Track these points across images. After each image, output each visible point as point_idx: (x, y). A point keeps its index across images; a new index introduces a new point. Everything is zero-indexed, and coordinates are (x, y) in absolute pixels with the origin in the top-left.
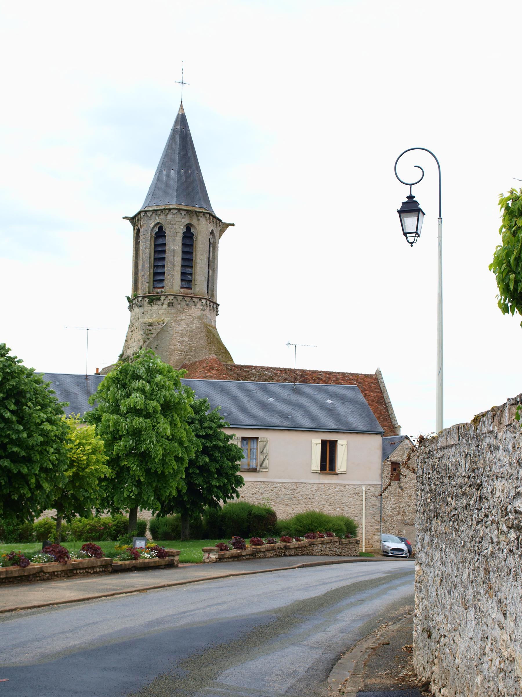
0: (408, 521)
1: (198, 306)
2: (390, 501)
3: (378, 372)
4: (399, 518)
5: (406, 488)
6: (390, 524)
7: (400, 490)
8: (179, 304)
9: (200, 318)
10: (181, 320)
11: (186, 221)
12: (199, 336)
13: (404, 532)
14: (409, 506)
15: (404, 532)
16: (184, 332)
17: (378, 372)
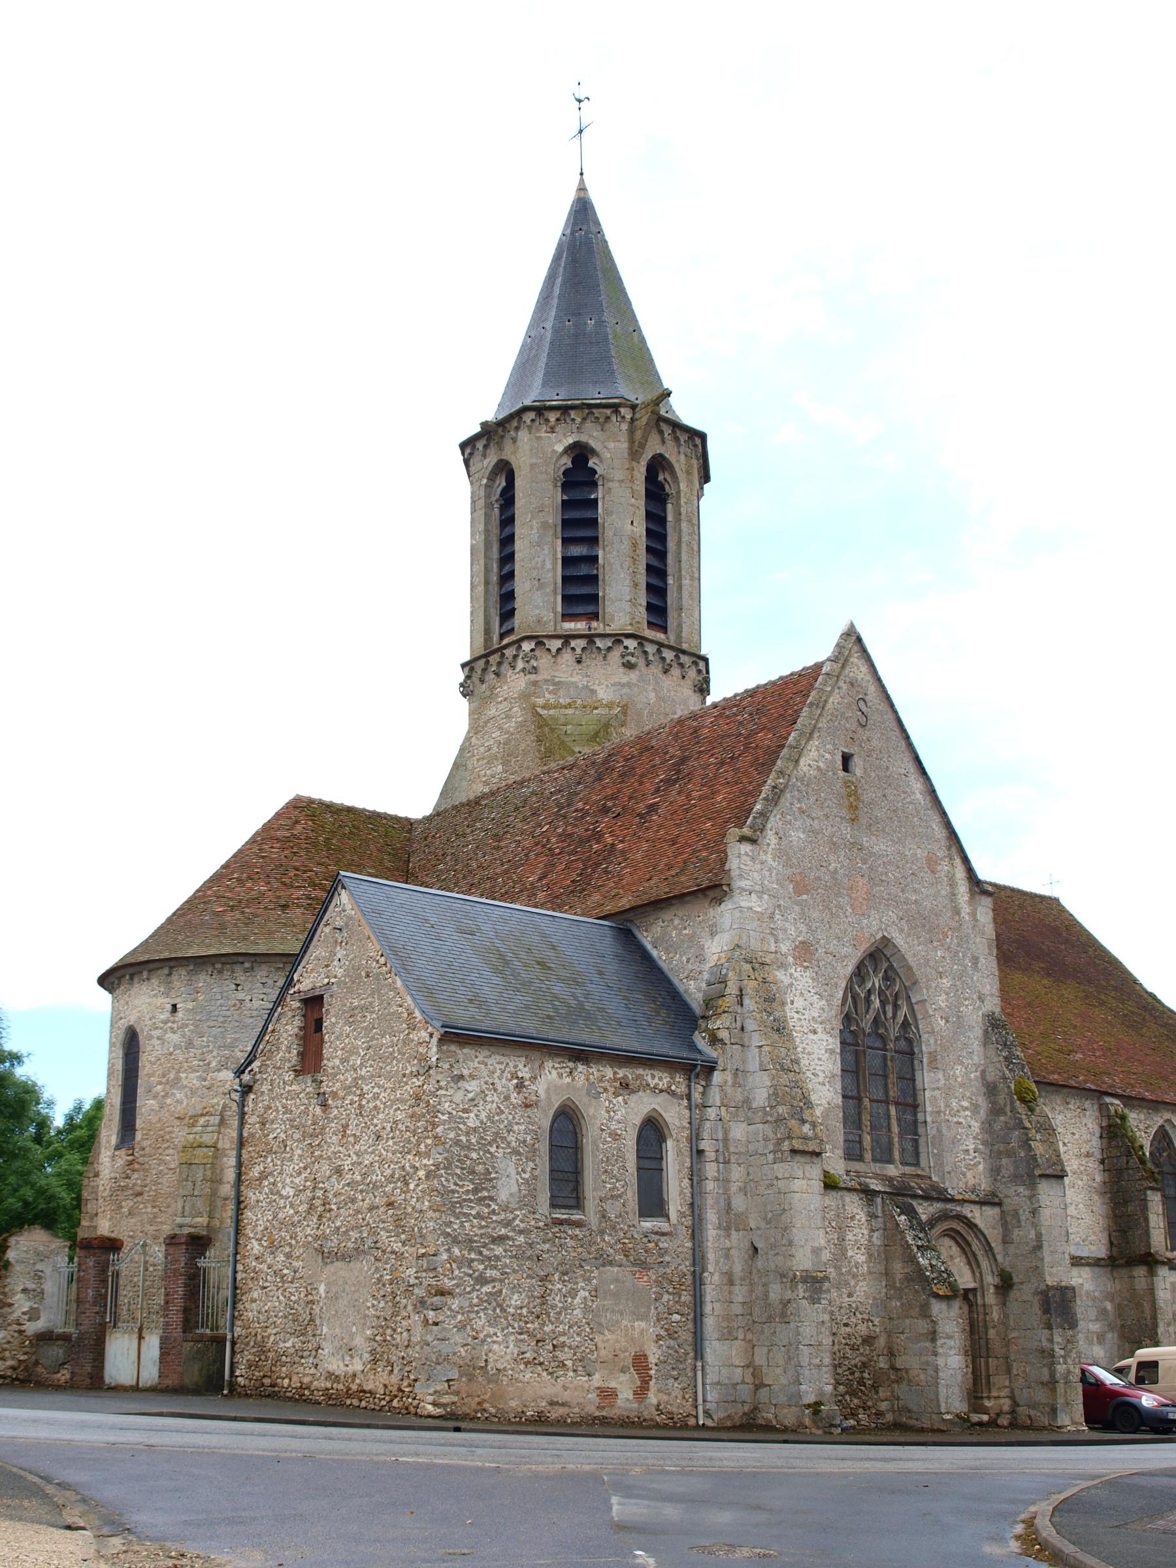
0: (332, 1244)
1: (520, 664)
2: (291, 1159)
3: (852, 643)
4: (309, 1230)
5: (334, 1095)
6: (288, 1256)
7: (318, 1110)
8: (482, 681)
9: (525, 696)
10: (486, 722)
11: (491, 461)
12: (523, 746)
13: (322, 1289)
14: (339, 1171)
15: (322, 1289)
16: (495, 749)
17: (852, 643)
